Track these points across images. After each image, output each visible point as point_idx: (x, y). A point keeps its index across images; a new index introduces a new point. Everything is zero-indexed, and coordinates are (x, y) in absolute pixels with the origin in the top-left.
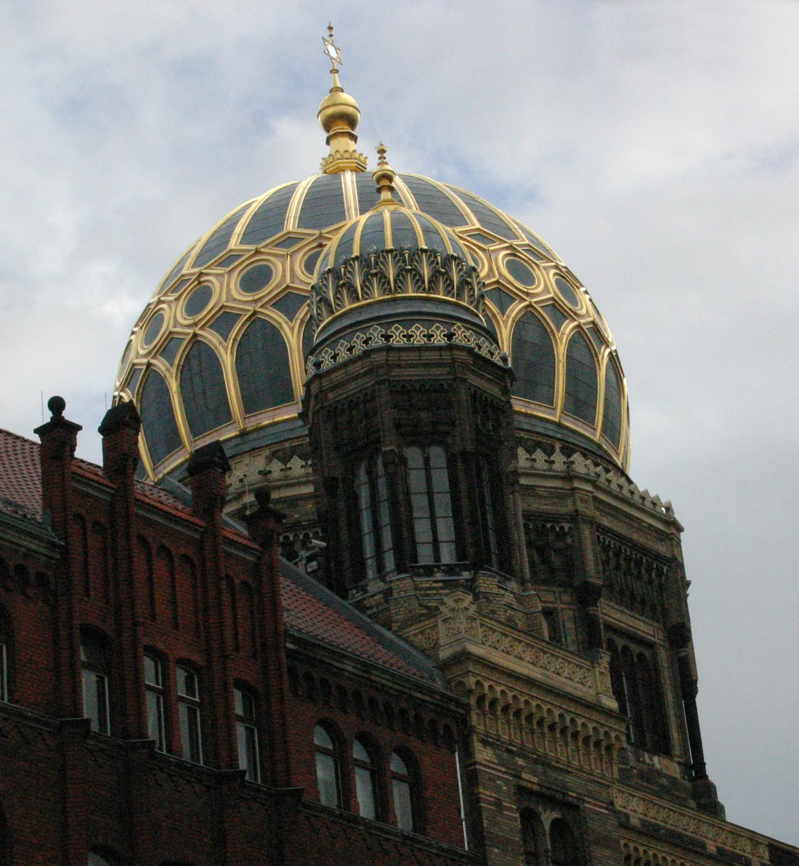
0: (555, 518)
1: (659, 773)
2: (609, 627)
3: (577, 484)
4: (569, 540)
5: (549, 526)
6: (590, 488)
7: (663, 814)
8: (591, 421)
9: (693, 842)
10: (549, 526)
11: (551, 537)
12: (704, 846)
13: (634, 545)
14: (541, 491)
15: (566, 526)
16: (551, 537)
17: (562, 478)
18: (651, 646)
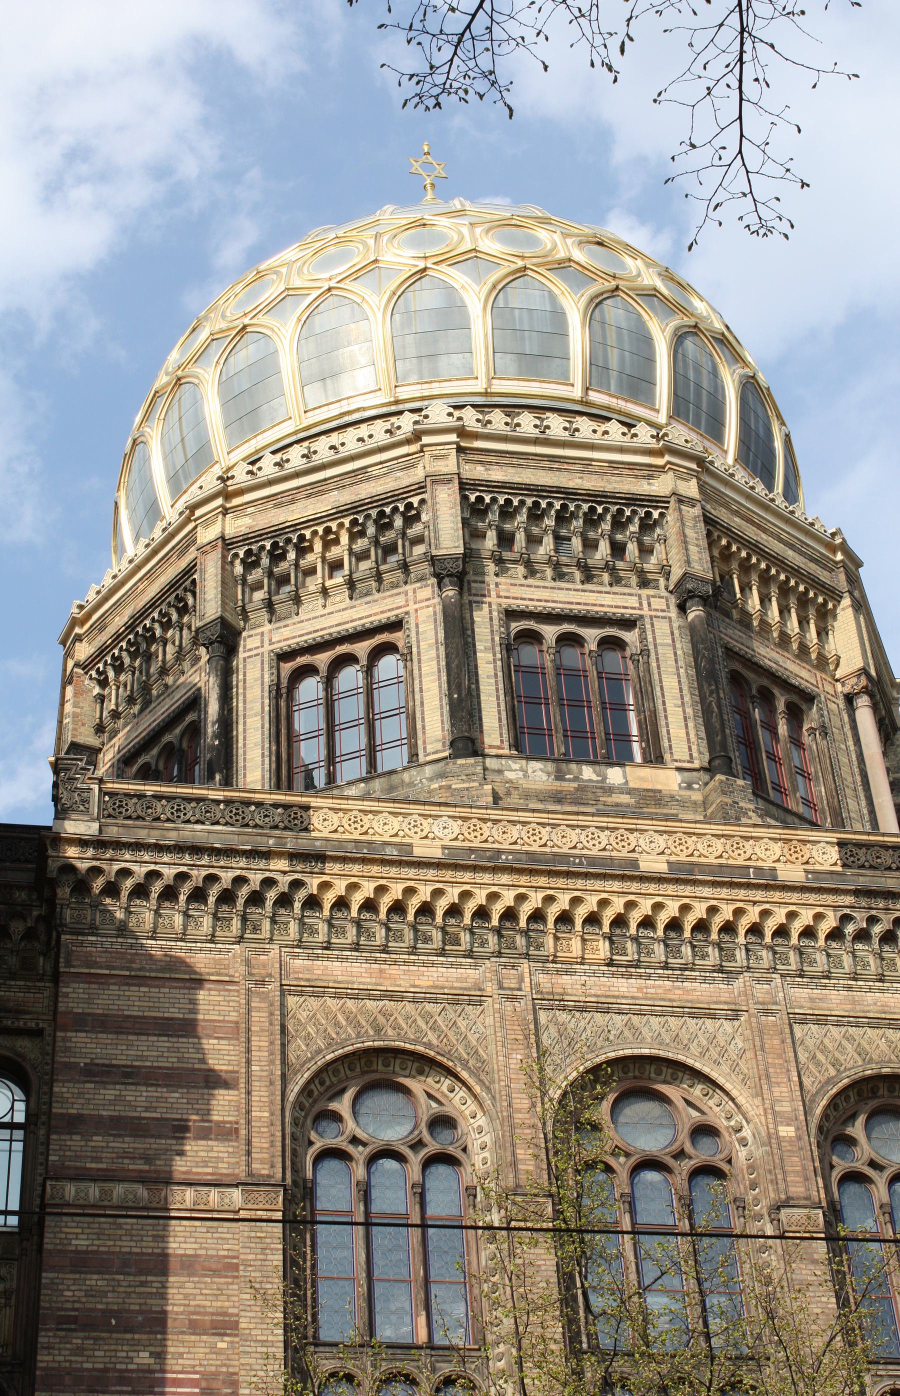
0: (394, 497)
1: (610, 790)
2: (511, 614)
3: (426, 440)
4: (424, 517)
5: (388, 510)
6: (453, 437)
7: (515, 832)
8: (565, 379)
9: (593, 861)
10: (388, 510)
11: (398, 522)
12: (634, 864)
13: (568, 494)
14: (374, 471)
15: (415, 501)
16: (398, 522)
17: (408, 442)
18: (628, 623)
